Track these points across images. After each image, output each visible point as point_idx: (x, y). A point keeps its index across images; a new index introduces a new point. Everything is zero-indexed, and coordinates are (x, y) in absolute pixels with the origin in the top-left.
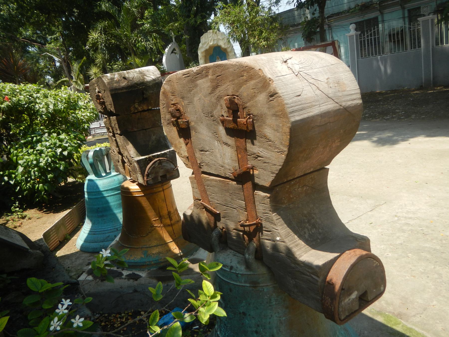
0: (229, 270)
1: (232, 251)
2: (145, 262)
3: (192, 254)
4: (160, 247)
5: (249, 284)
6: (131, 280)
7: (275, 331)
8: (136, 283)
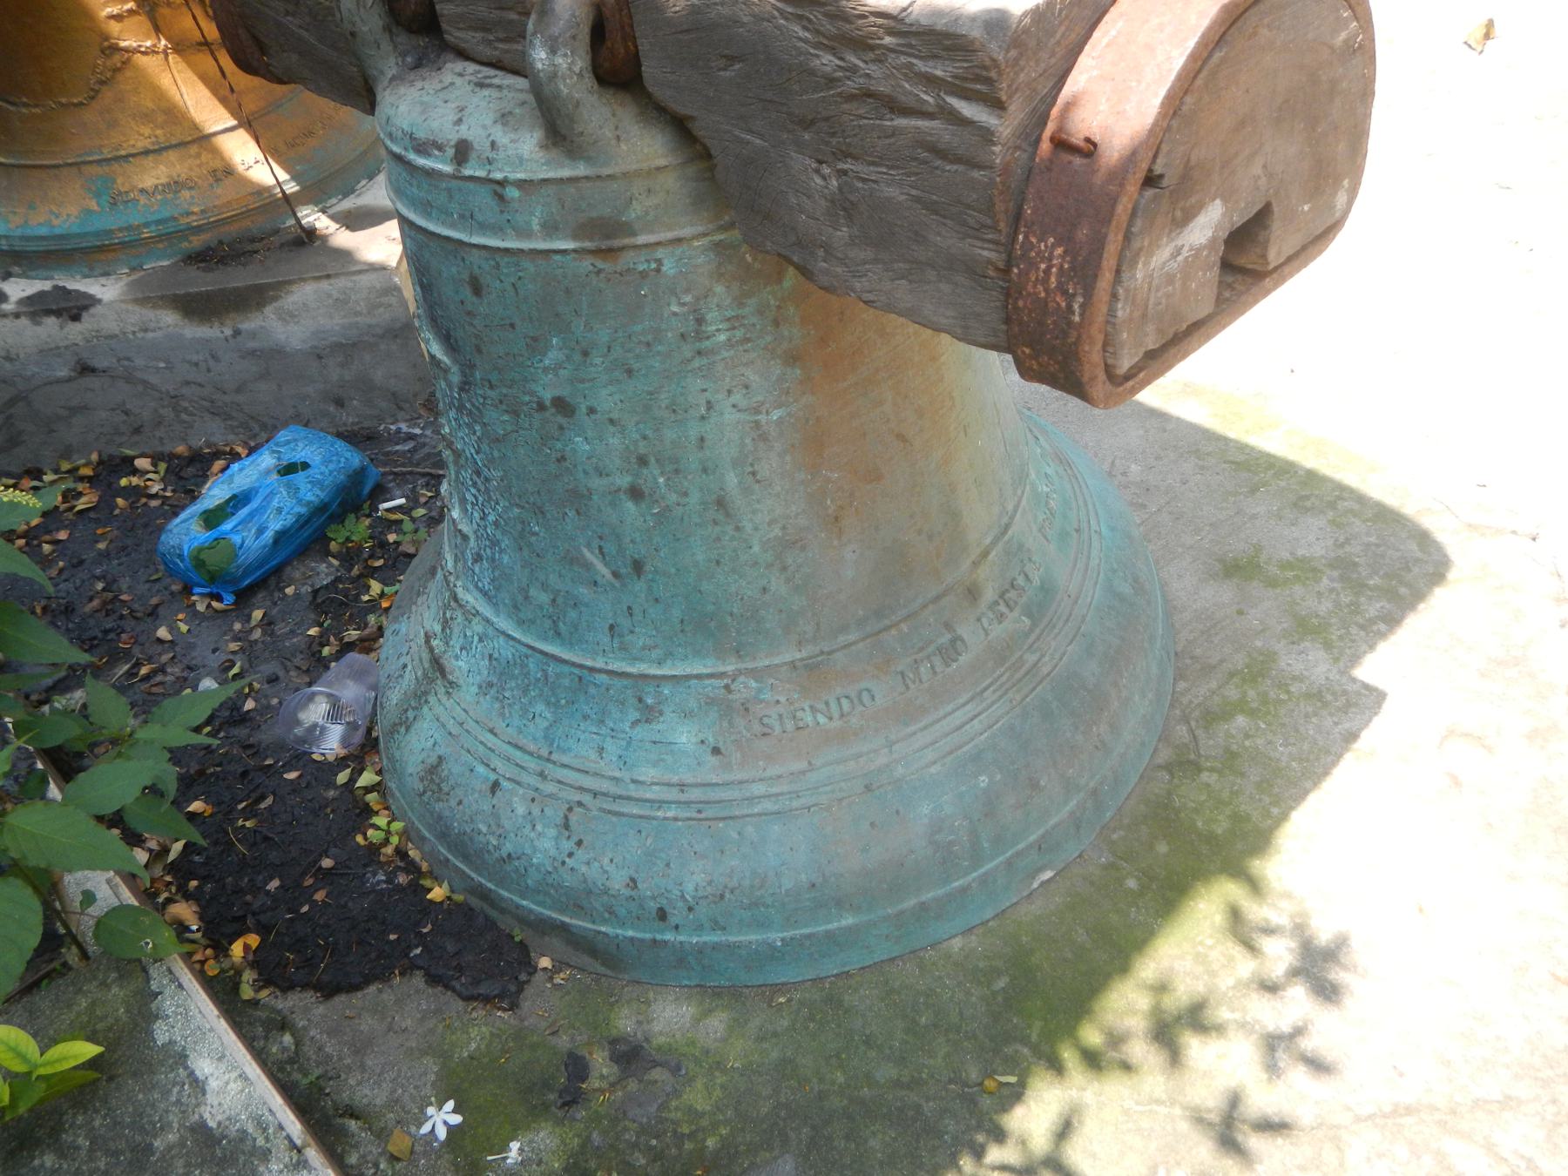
0: (447, 169)
1: (471, 67)
2: (109, 232)
3: (348, 192)
4: (172, 155)
5: (575, 237)
6: (51, 321)
7: (732, 480)
8: (75, 332)
